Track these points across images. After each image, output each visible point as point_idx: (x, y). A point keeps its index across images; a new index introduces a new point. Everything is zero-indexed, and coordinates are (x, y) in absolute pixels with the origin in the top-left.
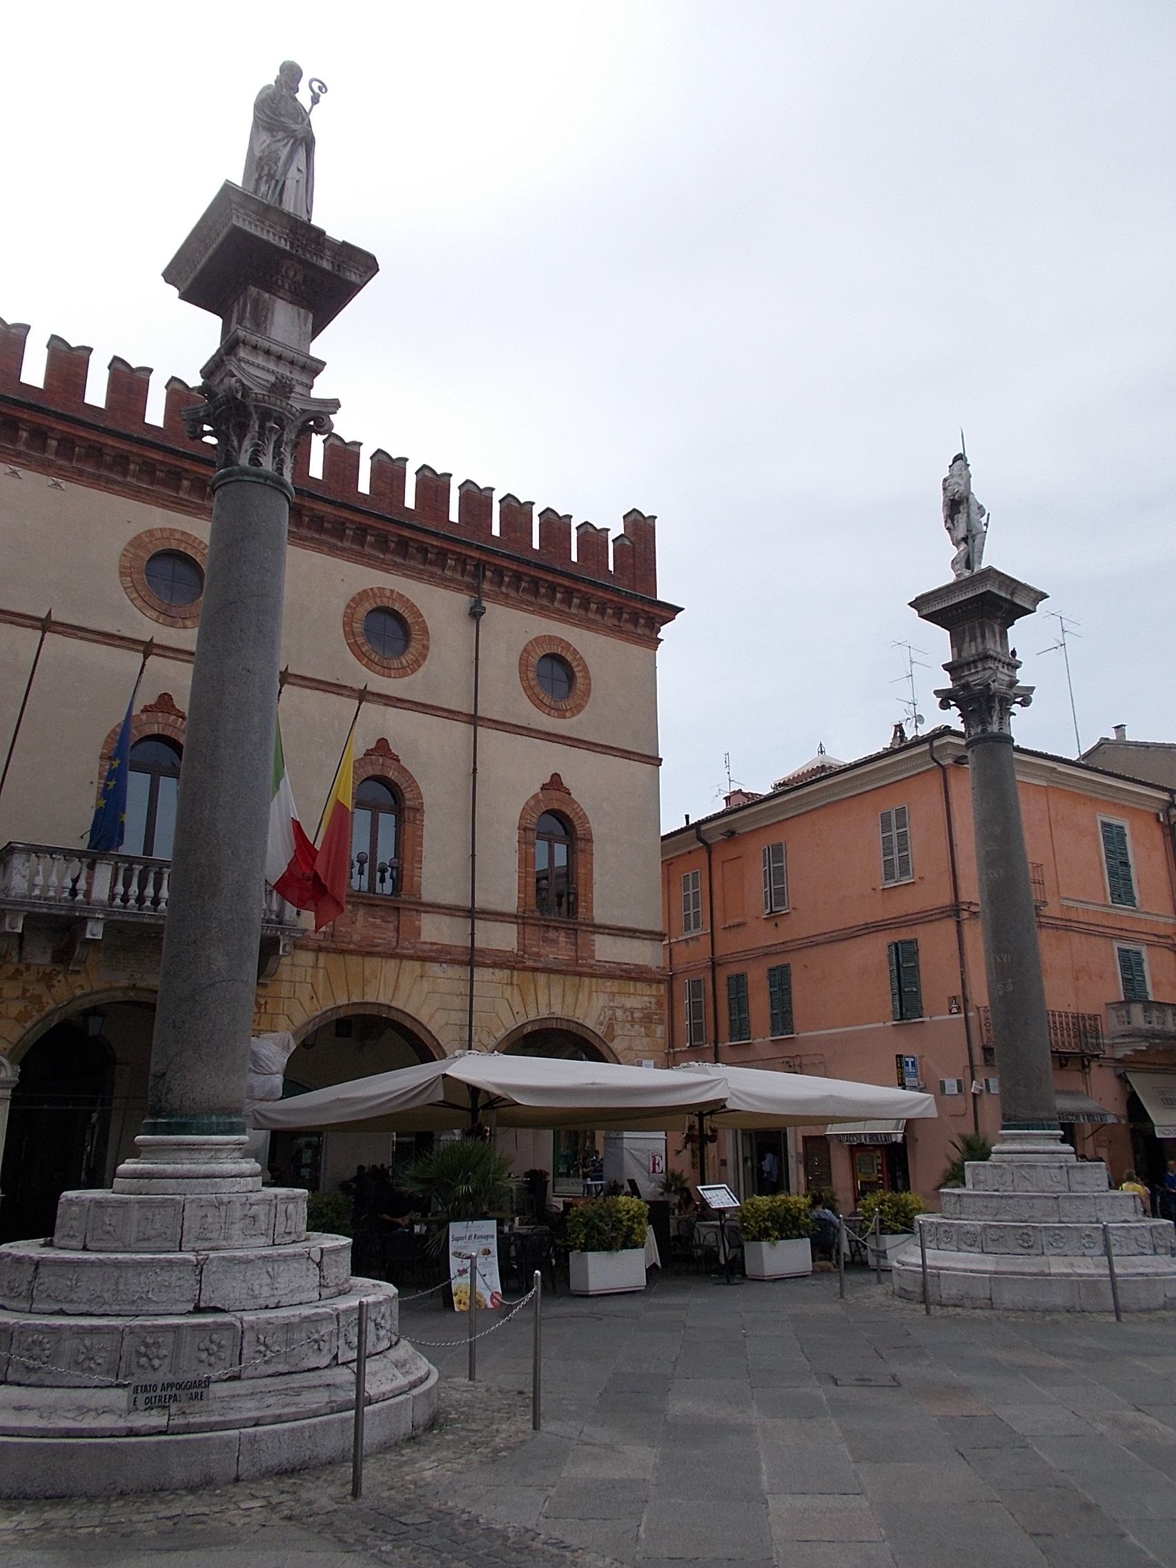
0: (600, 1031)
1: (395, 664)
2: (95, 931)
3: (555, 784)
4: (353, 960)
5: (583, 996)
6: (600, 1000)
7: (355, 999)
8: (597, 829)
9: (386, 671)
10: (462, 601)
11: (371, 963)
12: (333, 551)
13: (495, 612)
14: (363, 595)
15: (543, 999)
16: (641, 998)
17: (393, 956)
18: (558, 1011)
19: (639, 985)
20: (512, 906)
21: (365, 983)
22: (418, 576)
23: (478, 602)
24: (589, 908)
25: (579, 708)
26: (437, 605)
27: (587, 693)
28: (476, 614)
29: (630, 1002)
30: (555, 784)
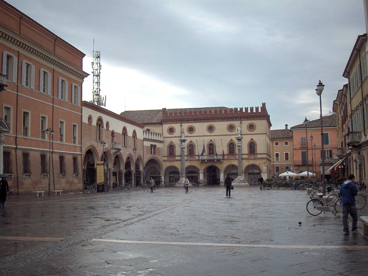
0: (258, 165)
1: (232, 131)
2: (206, 161)
3: (252, 139)
4: (230, 161)
5: (256, 161)
6: (259, 161)
7: (231, 164)
8: (257, 143)
9: (232, 132)
10: (240, 122)
11: (232, 160)
12: (225, 121)
13: (243, 122)
14: (228, 125)
15: (251, 162)
16: (264, 161)
17: (234, 160)
18: (253, 163)
19: (264, 160)
20: (247, 153)
21: (231, 162)
22: (234, 121)
23: (241, 122)
24: (257, 151)
25: (254, 130)
26: (236, 123)
27: (256, 128)
28: (241, 123)
29: (262, 161)
30: (252, 139)
